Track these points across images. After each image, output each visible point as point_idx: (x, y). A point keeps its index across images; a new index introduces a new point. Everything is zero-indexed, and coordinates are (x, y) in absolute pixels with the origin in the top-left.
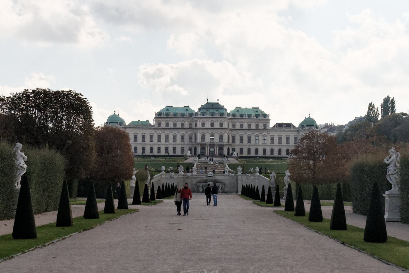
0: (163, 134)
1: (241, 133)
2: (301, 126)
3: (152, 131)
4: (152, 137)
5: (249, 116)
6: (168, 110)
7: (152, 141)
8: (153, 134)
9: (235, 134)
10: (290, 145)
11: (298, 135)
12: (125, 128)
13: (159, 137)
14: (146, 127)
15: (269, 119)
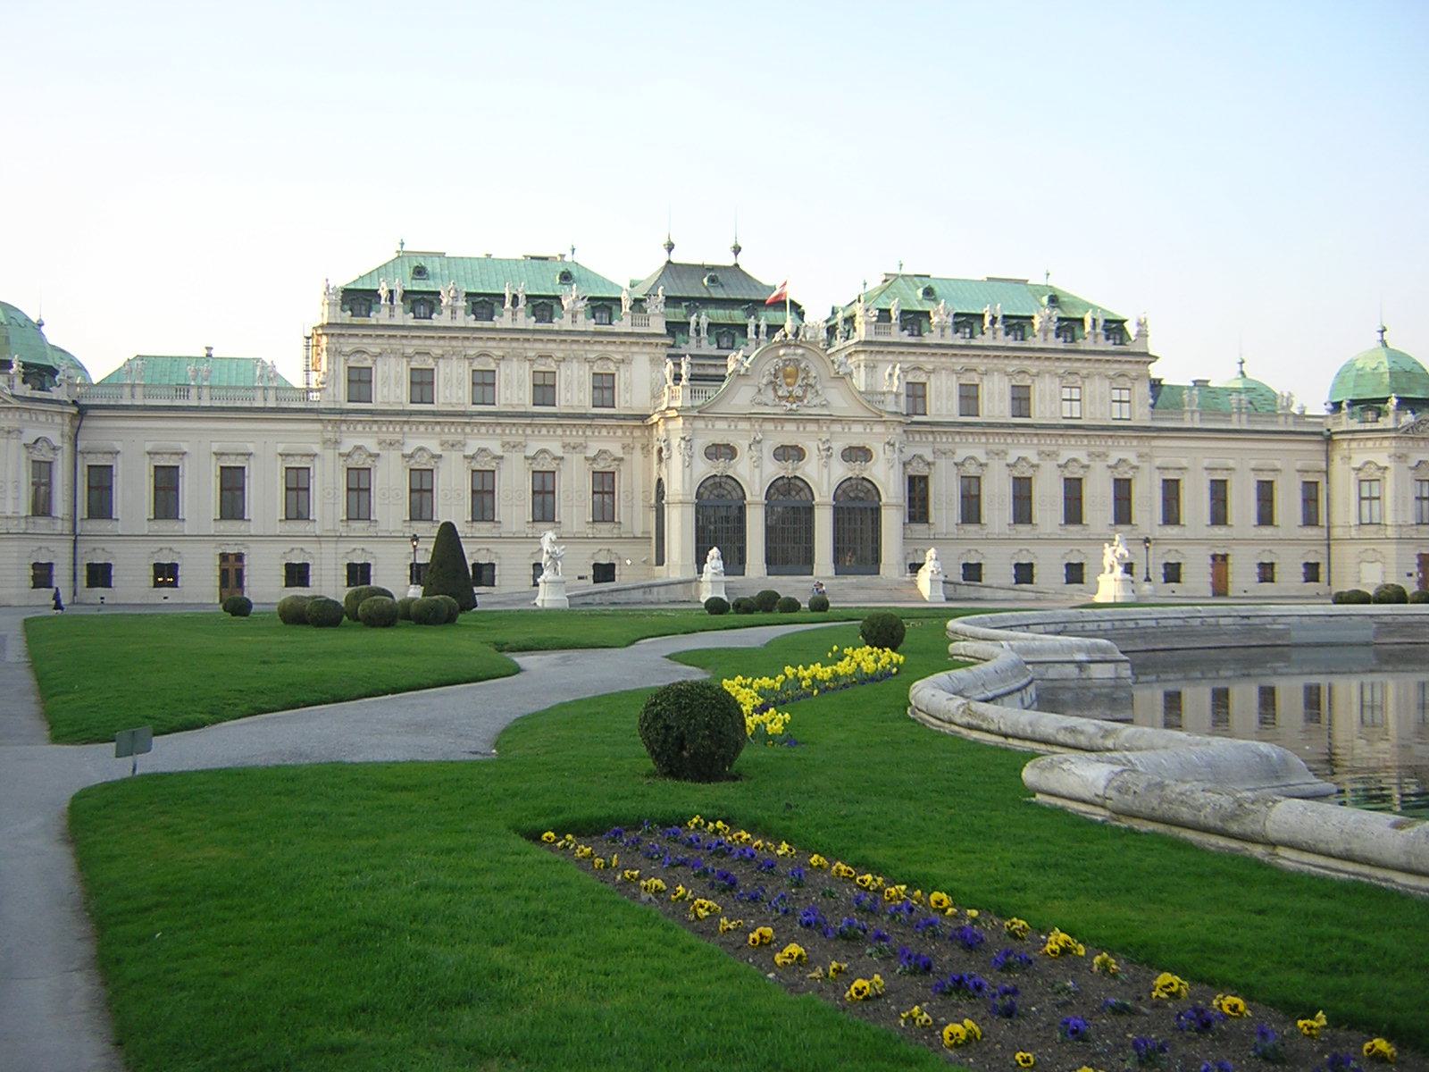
0: (454, 457)
1: (971, 449)
2: (1353, 403)
3: (304, 438)
4: (297, 487)
5: (1017, 324)
6: (420, 272)
7: (297, 509)
8: (315, 455)
9: (929, 457)
10: (1281, 533)
11: (1323, 466)
12: (74, 410)
13: (359, 488)
14: (247, 404)
15: (1146, 354)
